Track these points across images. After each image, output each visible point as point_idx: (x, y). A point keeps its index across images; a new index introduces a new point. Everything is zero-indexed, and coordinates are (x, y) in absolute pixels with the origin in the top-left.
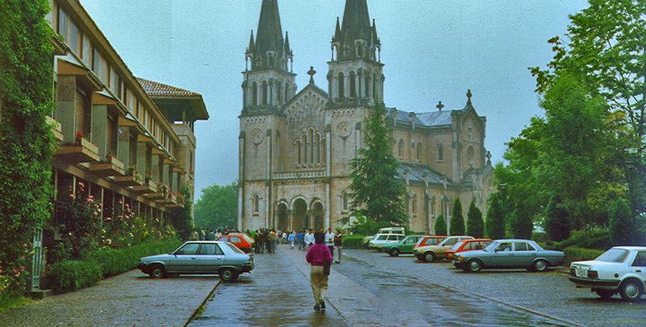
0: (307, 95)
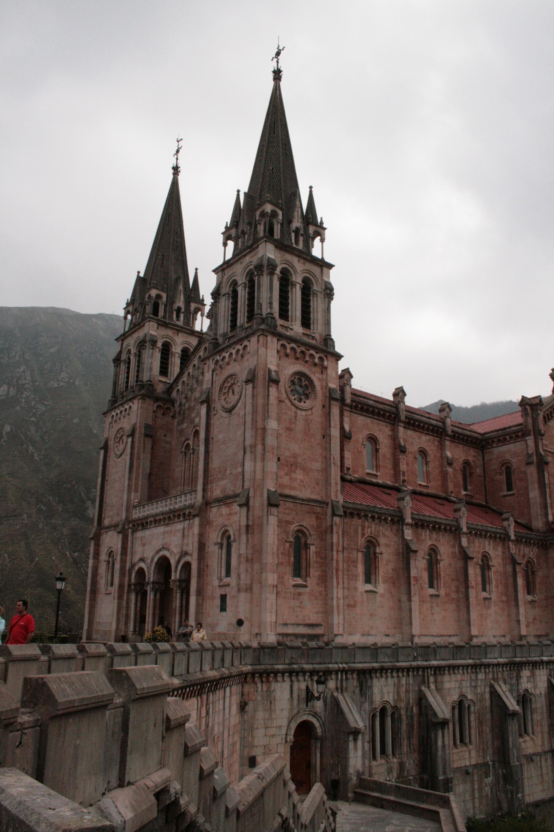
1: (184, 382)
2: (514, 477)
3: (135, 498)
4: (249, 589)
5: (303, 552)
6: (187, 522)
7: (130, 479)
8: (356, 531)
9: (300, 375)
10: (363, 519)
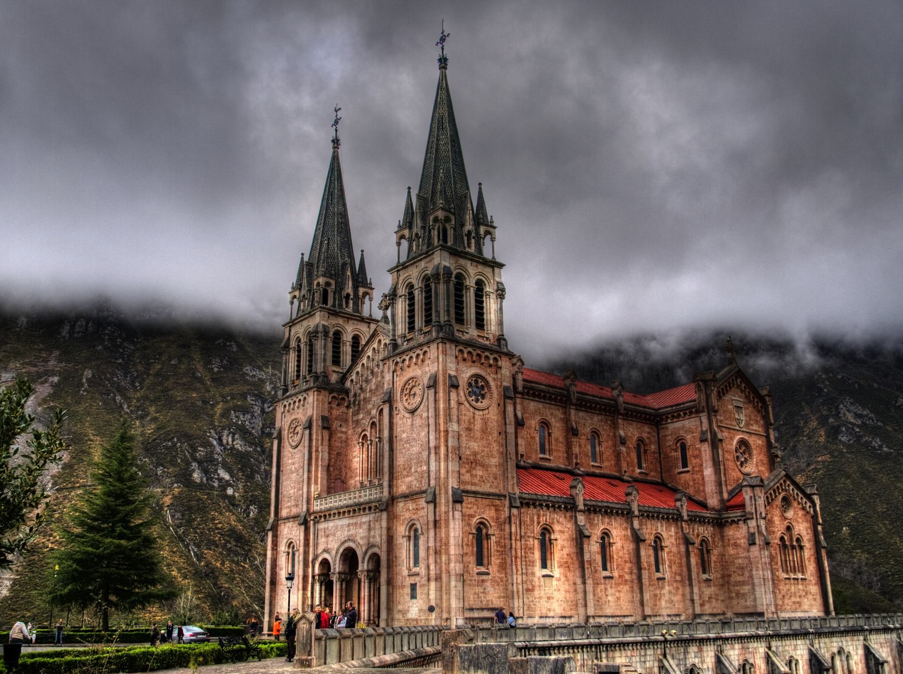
0: (375, 346)
1: (358, 373)
2: (689, 453)
3: (315, 489)
4: (438, 578)
5: (485, 542)
6: (372, 515)
7: (309, 471)
8: (532, 521)
9: (477, 376)
10: (539, 508)
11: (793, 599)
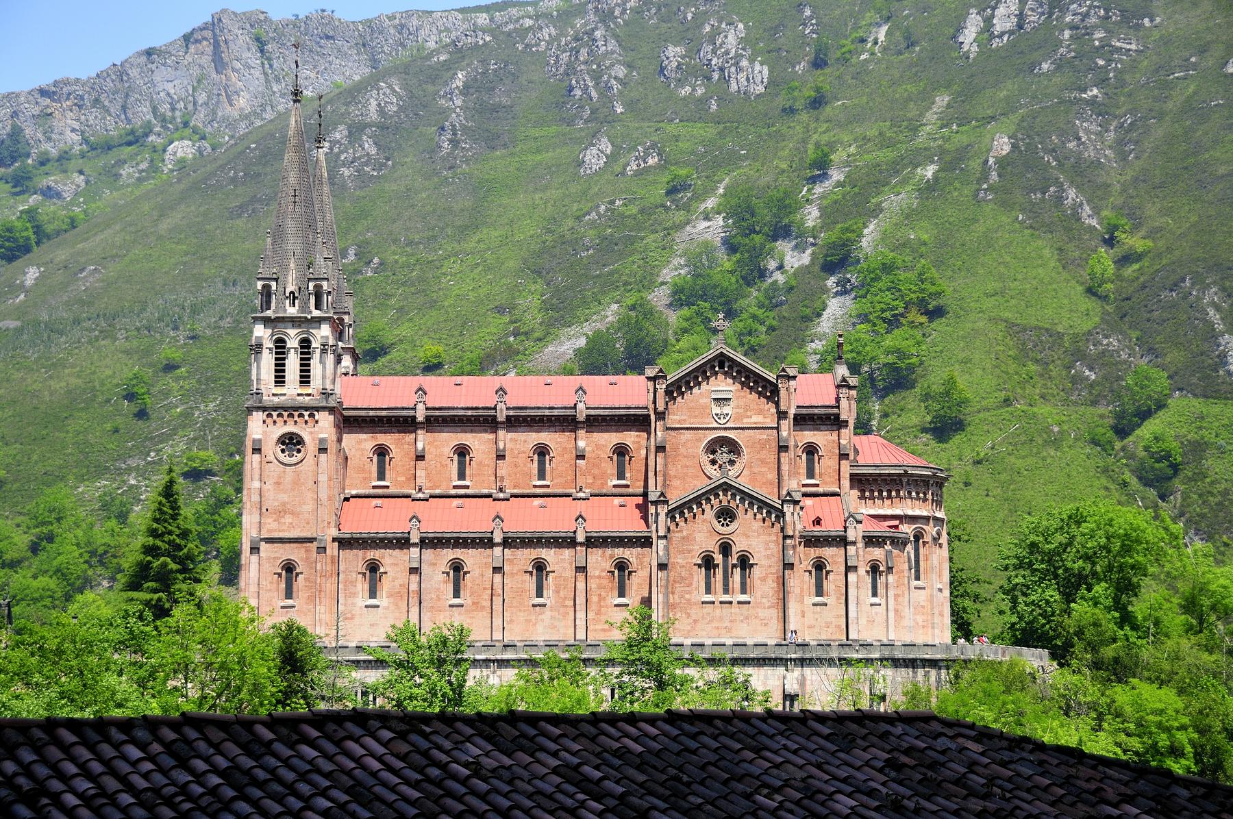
11: (716, 624)
